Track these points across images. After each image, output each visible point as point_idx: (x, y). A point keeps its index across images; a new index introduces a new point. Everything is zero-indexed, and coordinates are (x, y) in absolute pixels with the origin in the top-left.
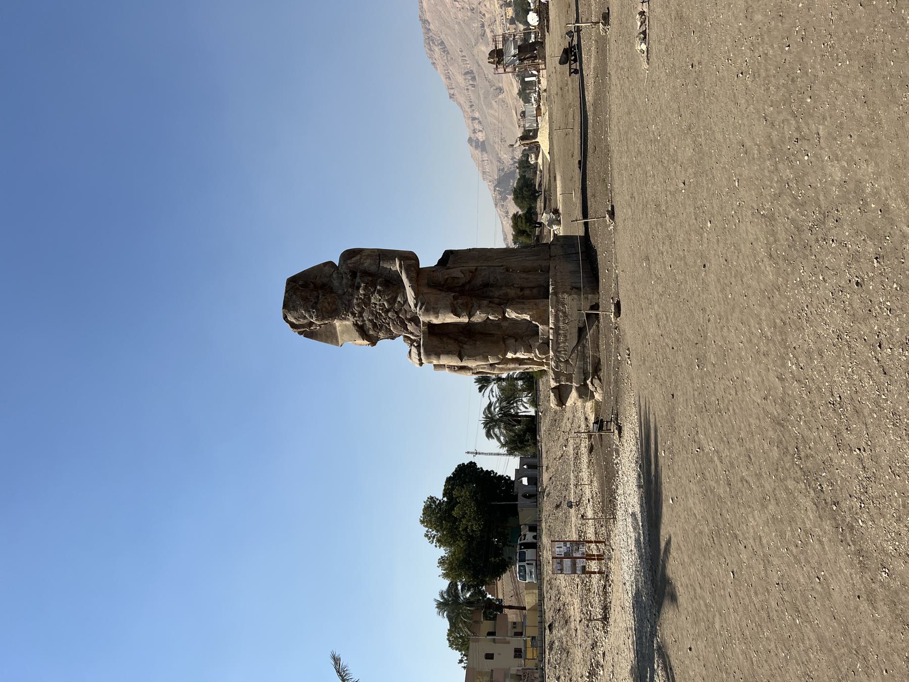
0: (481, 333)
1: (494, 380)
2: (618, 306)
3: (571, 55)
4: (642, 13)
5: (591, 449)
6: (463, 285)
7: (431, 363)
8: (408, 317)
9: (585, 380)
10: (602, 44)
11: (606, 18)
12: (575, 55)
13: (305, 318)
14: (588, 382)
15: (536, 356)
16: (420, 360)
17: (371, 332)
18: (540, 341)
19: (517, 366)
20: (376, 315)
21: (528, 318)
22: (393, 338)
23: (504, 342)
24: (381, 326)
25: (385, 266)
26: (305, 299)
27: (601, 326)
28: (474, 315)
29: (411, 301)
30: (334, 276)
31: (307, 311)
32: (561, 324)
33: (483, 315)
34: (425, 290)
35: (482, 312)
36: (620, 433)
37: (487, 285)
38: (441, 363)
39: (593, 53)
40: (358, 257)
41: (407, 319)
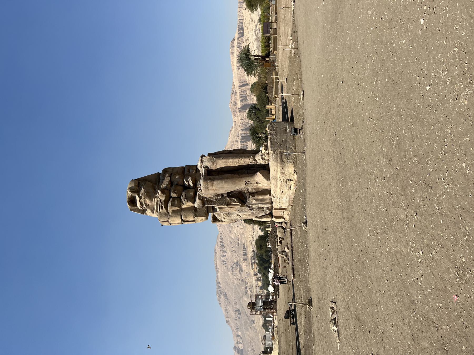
3: (291, 314)
4: (332, 308)
10: (308, 316)
11: (310, 302)
12: (293, 314)
39: (303, 318)
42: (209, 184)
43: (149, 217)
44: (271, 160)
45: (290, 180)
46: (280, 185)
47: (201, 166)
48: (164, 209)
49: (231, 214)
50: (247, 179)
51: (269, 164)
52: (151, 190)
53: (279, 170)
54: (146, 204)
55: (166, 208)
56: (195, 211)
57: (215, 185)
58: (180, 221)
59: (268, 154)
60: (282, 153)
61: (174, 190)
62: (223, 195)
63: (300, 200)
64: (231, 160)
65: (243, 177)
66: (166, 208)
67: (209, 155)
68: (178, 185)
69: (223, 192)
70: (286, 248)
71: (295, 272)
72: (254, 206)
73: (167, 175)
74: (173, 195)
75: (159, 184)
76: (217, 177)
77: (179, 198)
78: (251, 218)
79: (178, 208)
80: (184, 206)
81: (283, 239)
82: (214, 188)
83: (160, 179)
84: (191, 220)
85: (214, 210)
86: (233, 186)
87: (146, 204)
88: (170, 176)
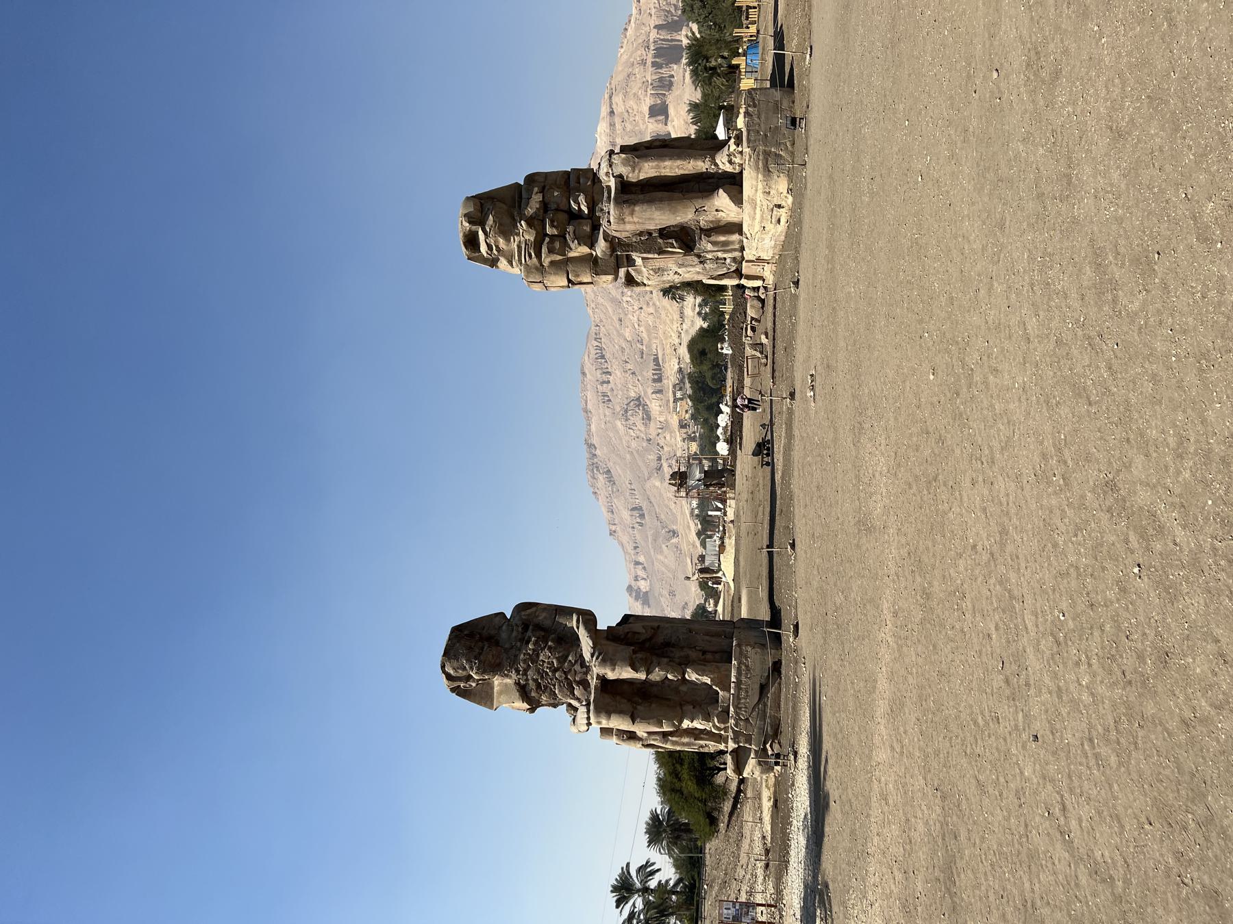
0: (656, 697)
1: (638, 891)
2: (796, 627)
3: (764, 449)
5: (767, 866)
6: (644, 642)
7: (599, 723)
9: (765, 743)
15: (714, 726)
16: (588, 718)
17: (533, 694)
20: (542, 674)
21: (709, 681)
22: (555, 706)
24: (546, 687)
25: (561, 620)
26: (470, 649)
29: (587, 655)
32: (743, 679)
33: (662, 673)
34: (604, 642)
35: (662, 669)
36: (795, 757)
37: (667, 644)
38: (611, 726)
40: (534, 609)
42: (627, 211)
43: (505, 272)
44: (746, 166)
45: (779, 206)
46: (759, 216)
47: (607, 174)
48: (535, 260)
49: (663, 270)
50: (698, 203)
51: (741, 173)
52: (507, 220)
53: (760, 186)
54: (497, 247)
55: (539, 256)
56: (594, 264)
57: (636, 214)
58: (565, 283)
59: (741, 153)
60: (767, 154)
61: (552, 222)
62: (650, 234)
63: (791, 244)
64: (668, 163)
65: (691, 199)
66: (539, 256)
67: (624, 149)
68: (557, 210)
69: (651, 227)
70: (763, 337)
71: (777, 374)
72: (709, 256)
73: (536, 189)
74: (549, 230)
75: (520, 206)
76: (641, 197)
77: (562, 236)
78: (699, 278)
79: (559, 258)
80: (572, 254)
81: (758, 321)
82: (636, 220)
83: (520, 197)
84: (585, 280)
85: (631, 262)
86: (672, 216)
87: (497, 247)
88: (542, 191)
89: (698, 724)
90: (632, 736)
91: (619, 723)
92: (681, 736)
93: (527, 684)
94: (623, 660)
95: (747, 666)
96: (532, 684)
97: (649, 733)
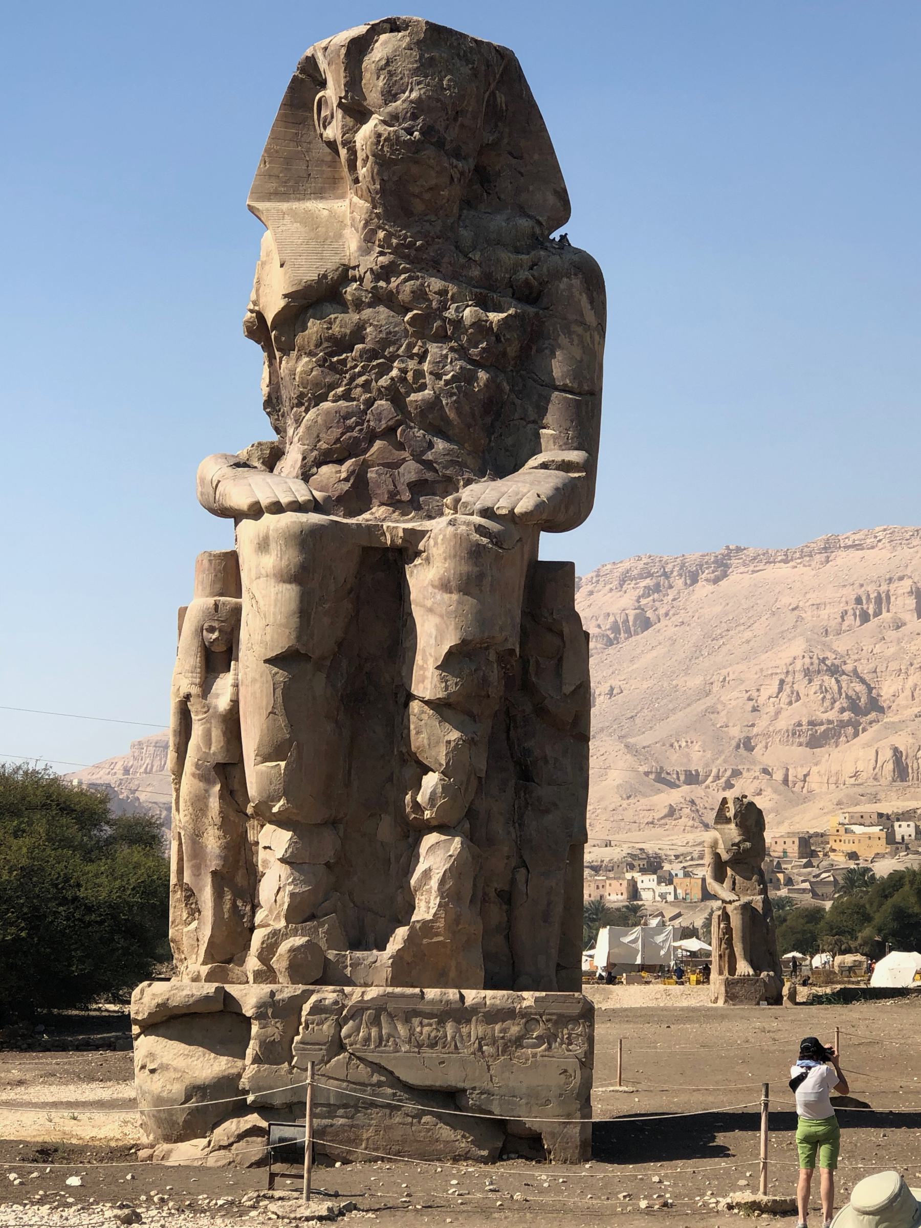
6: (527, 687)
7: (263, 545)
8: (372, 474)
9: (264, 1108)
13: (390, 95)
14: (253, 1120)
16: (277, 508)
17: (314, 327)
18: (331, 954)
19: (214, 864)
20: (380, 355)
22: (272, 404)
23: (324, 824)
27: (467, 1168)
28: (444, 719)
30: (524, 223)
31: (418, 108)
32: (475, 1029)
33: (441, 755)
35: (455, 751)
40: (590, 317)
41: (364, 467)
89: (275, 884)
90: (217, 655)
91: (266, 612)
92: (225, 824)
93: (343, 307)
94: (482, 619)
95: (518, 1042)
96: (342, 322)
97: (231, 722)
